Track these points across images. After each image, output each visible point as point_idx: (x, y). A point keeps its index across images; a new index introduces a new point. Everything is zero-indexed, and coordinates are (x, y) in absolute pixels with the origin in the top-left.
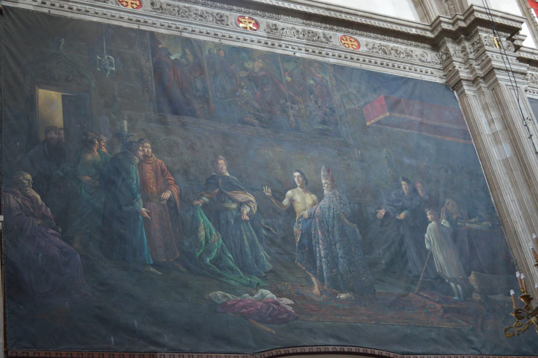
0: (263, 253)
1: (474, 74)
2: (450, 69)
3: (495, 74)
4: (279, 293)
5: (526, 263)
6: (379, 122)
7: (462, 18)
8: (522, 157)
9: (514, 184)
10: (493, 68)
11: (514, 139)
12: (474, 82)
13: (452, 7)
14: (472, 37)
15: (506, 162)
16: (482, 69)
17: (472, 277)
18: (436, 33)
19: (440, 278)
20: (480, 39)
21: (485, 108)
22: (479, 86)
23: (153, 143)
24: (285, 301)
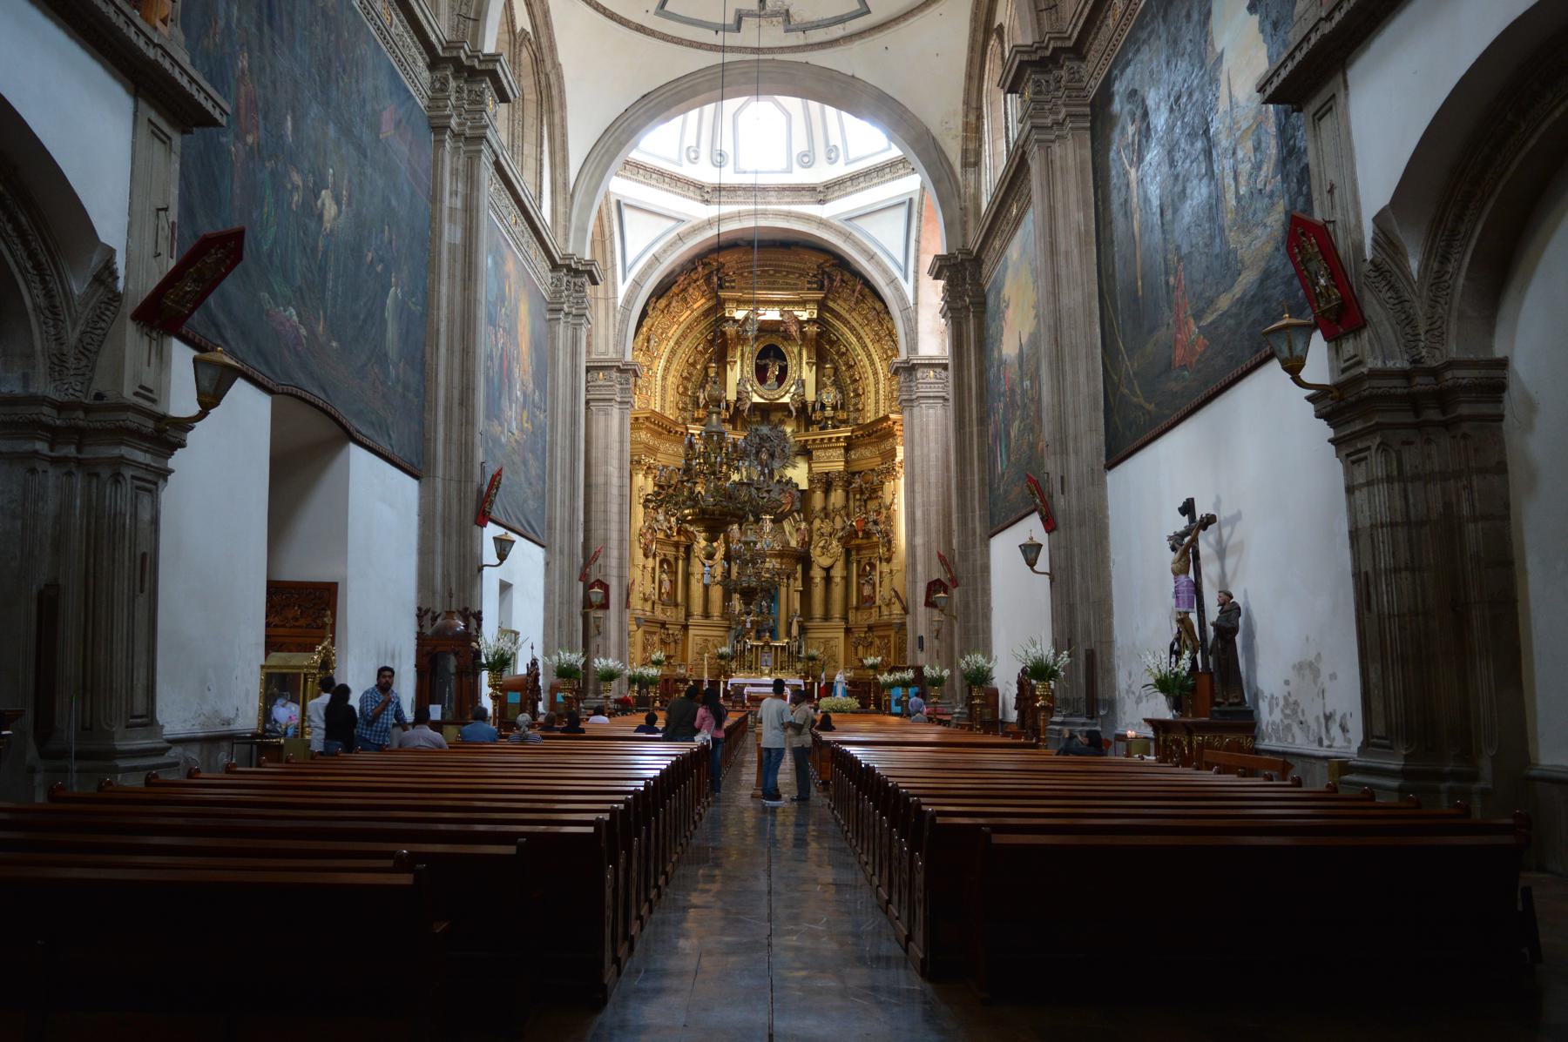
0: (297, 261)
1: (462, 128)
2: (441, 104)
3: (481, 144)
4: (299, 315)
5: (437, 369)
6: (387, 138)
7: (481, 58)
8: (470, 253)
9: (452, 276)
10: (485, 137)
11: (471, 228)
12: (456, 136)
13: (462, 26)
14: (475, 82)
15: (452, 247)
16: (470, 128)
17: (401, 365)
18: (447, 55)
19: (386, 355)
20: (482, 92)
21: (454, 172)
22: (457, 145)
23: (250, 57)
24: (303, 331)
